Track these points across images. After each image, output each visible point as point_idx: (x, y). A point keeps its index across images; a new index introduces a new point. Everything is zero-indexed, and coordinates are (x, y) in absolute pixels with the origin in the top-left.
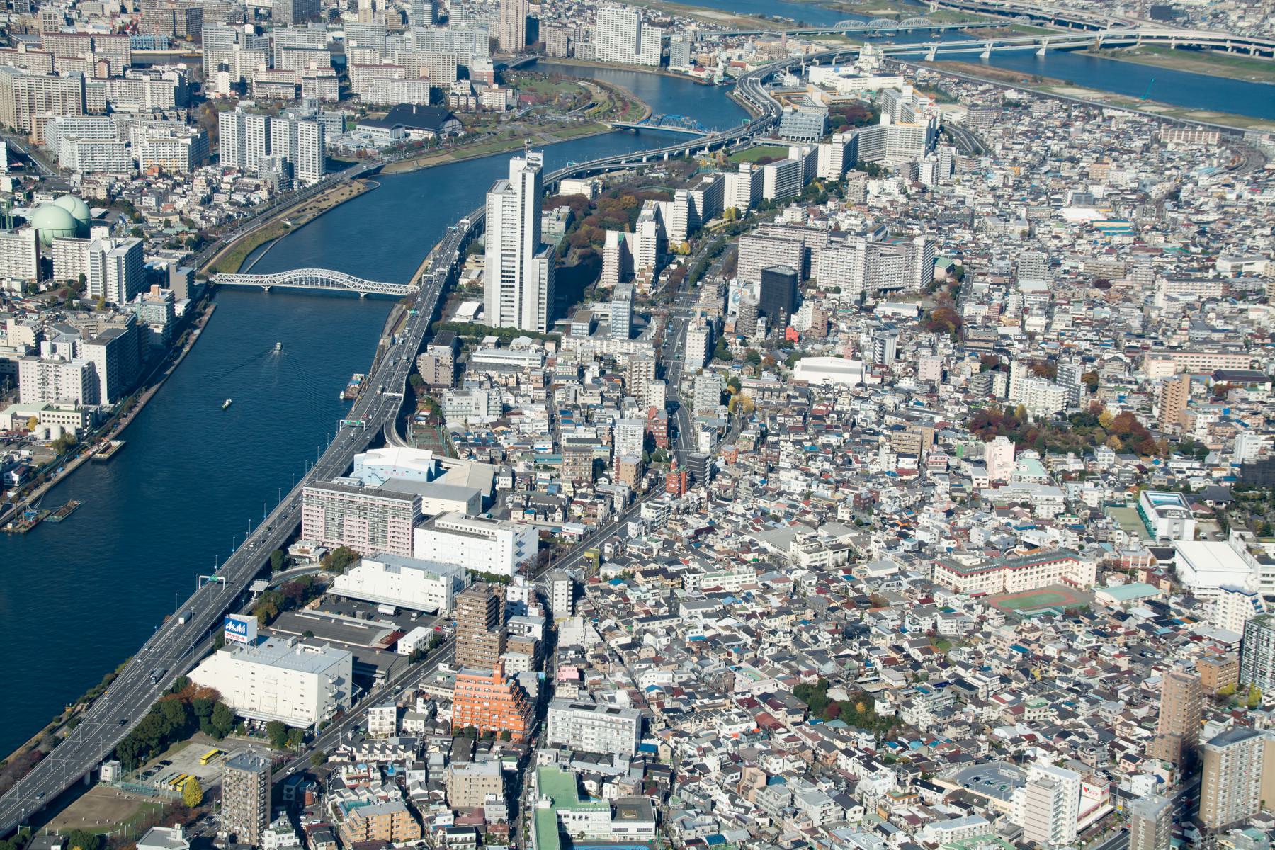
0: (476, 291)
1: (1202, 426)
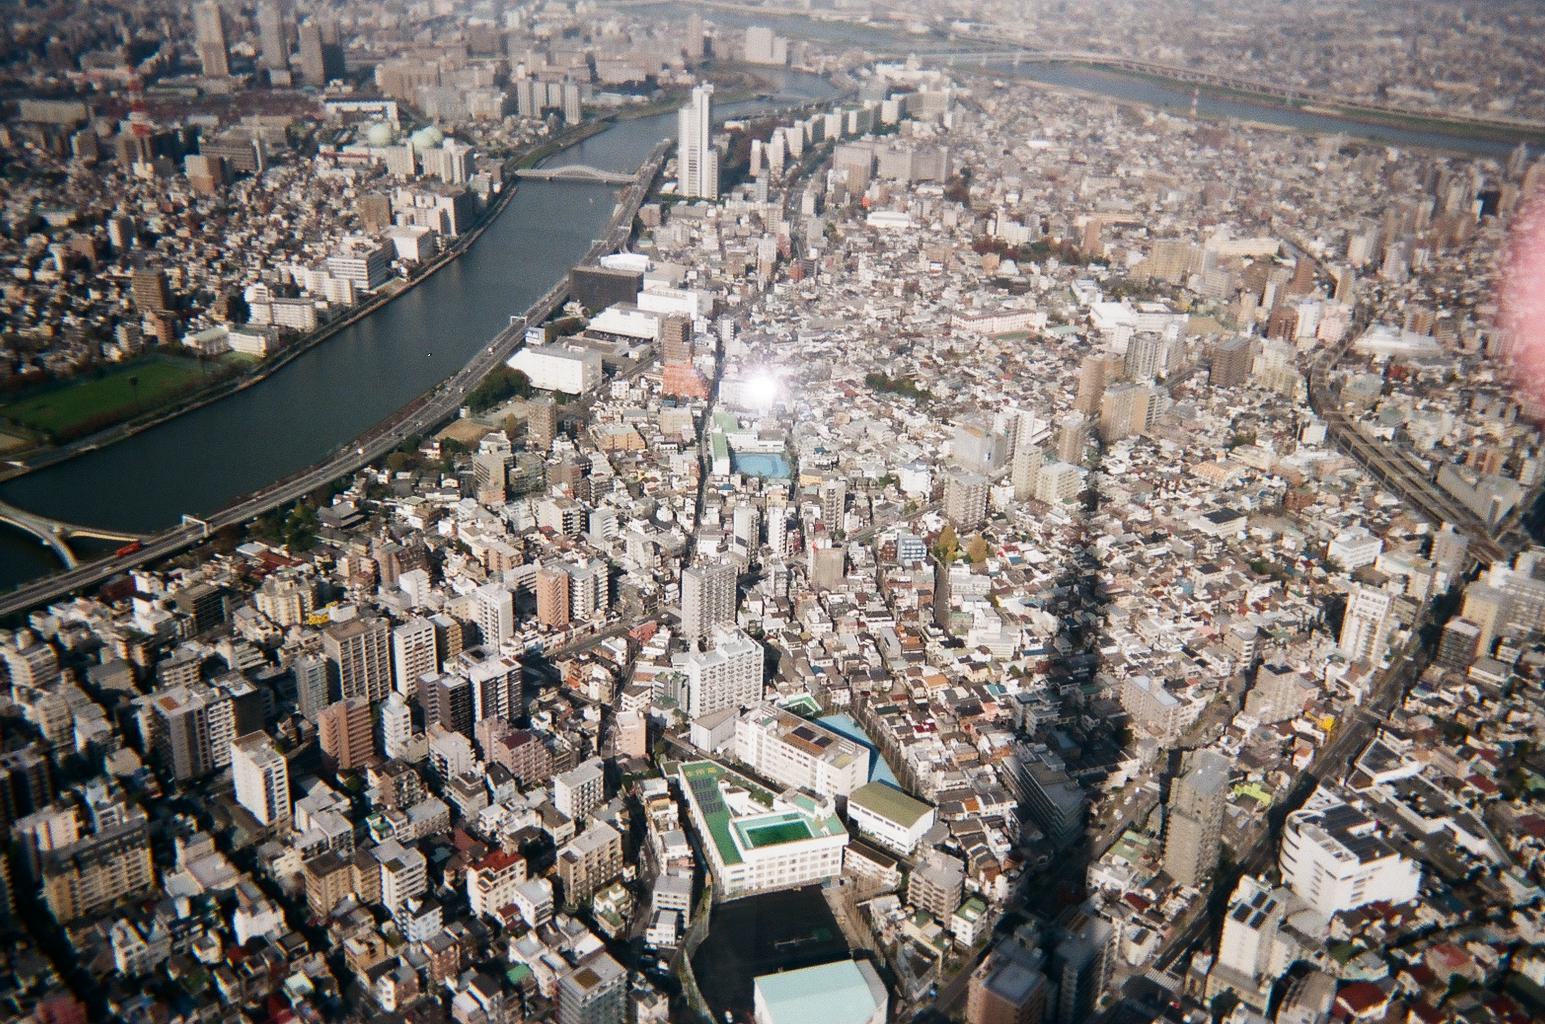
1: (1107, 249)
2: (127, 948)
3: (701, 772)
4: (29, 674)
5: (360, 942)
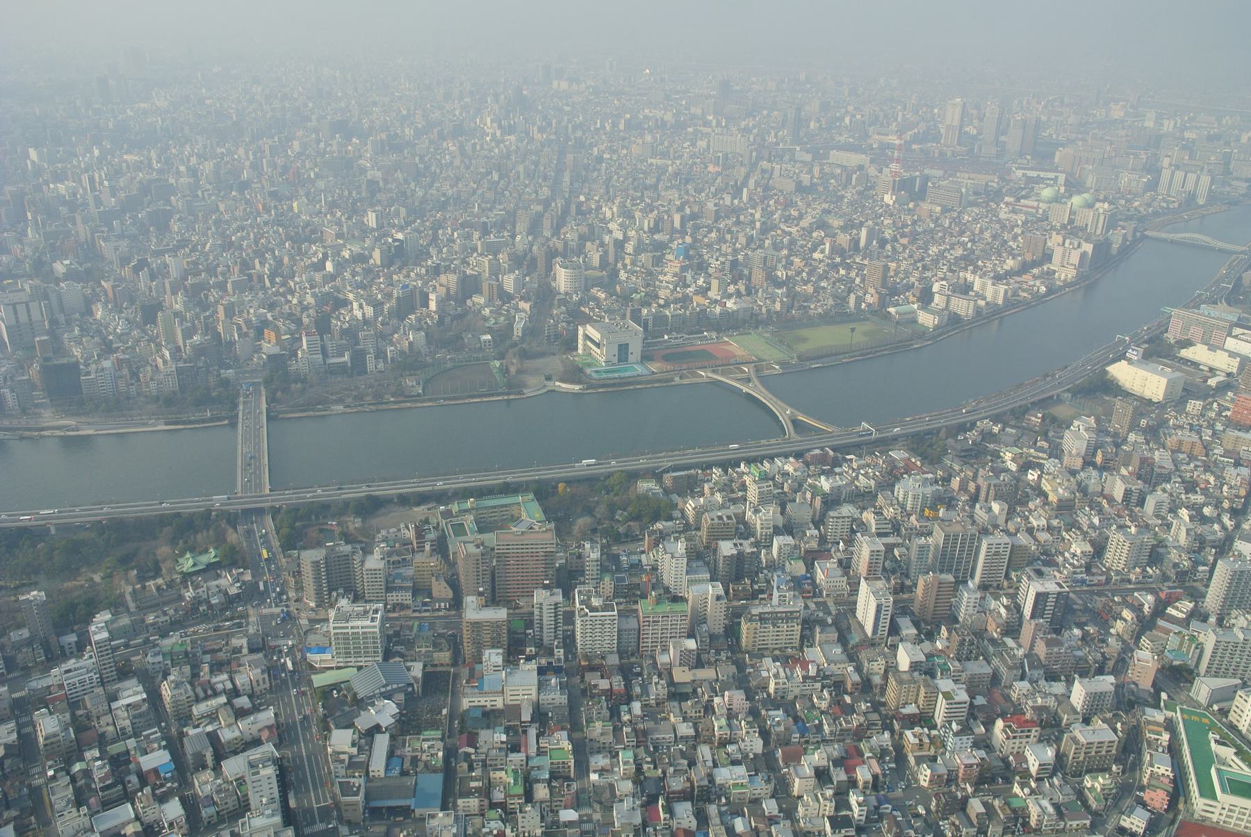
3: (1196, 719)
5: (915, 736)
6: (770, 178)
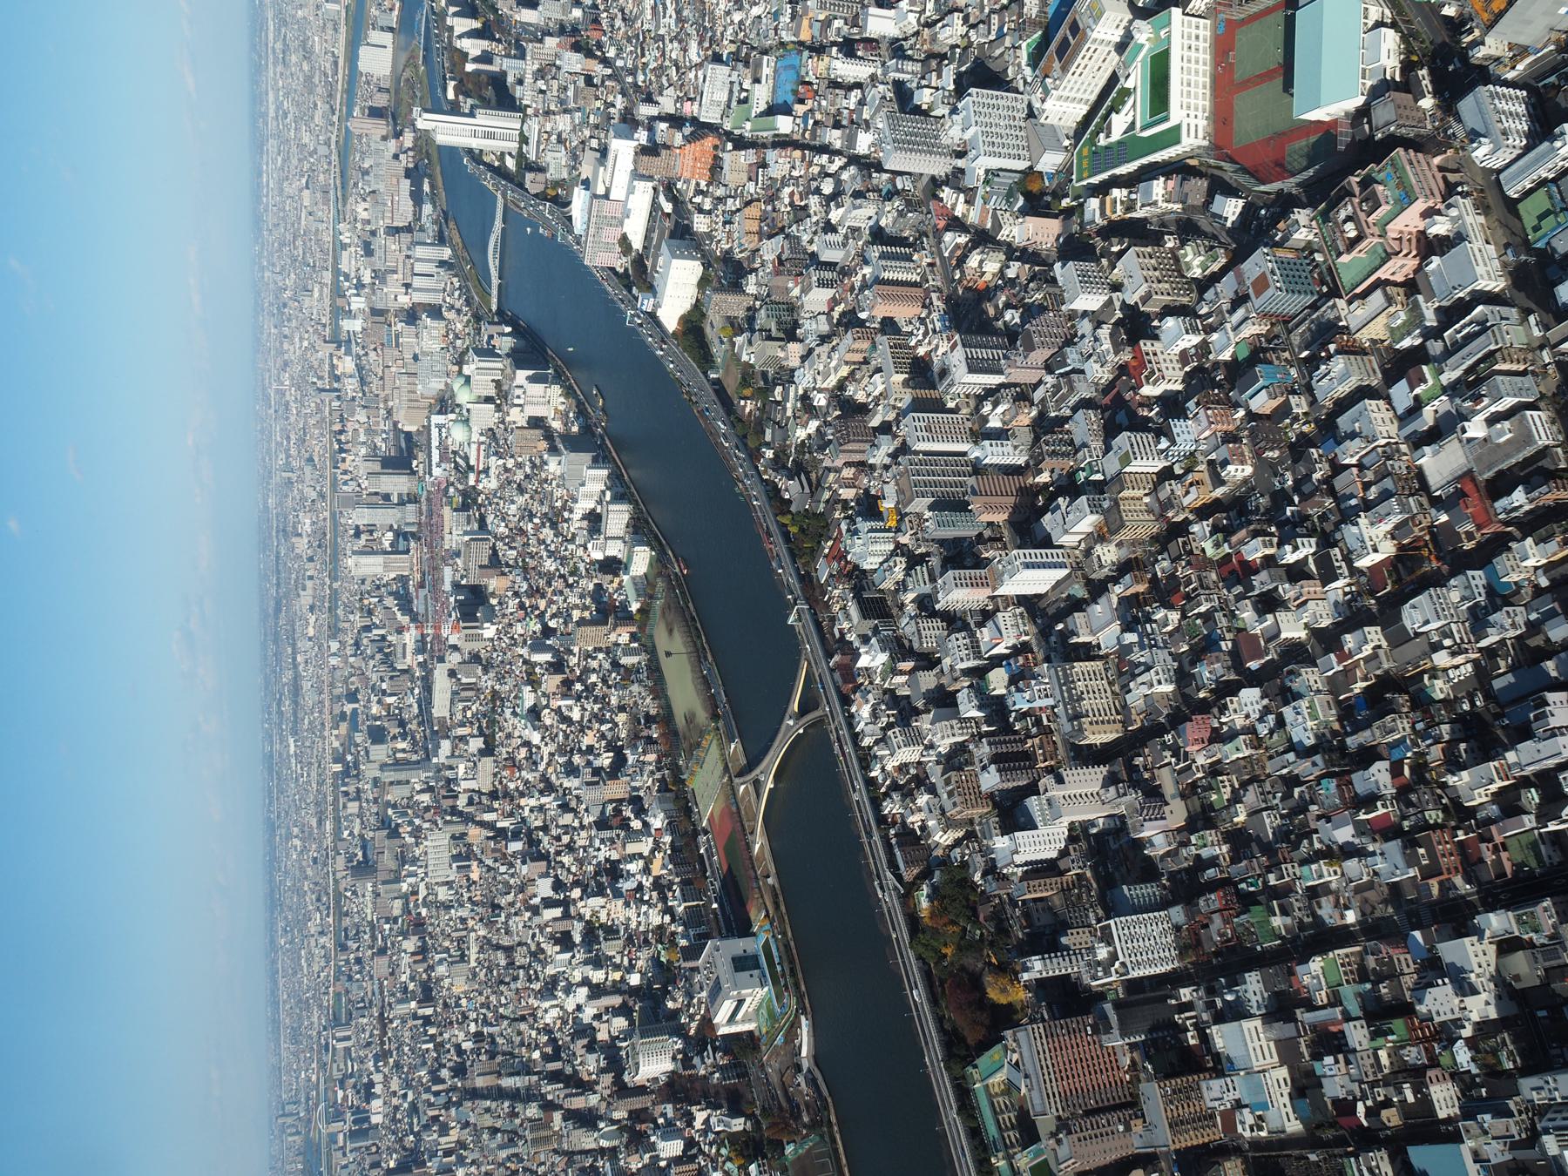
0: (502, 157)
2: (1155, 683)
3: (1085, 162)
4: (912, 748)
5: (1187, 493)
6: (480, 793)
